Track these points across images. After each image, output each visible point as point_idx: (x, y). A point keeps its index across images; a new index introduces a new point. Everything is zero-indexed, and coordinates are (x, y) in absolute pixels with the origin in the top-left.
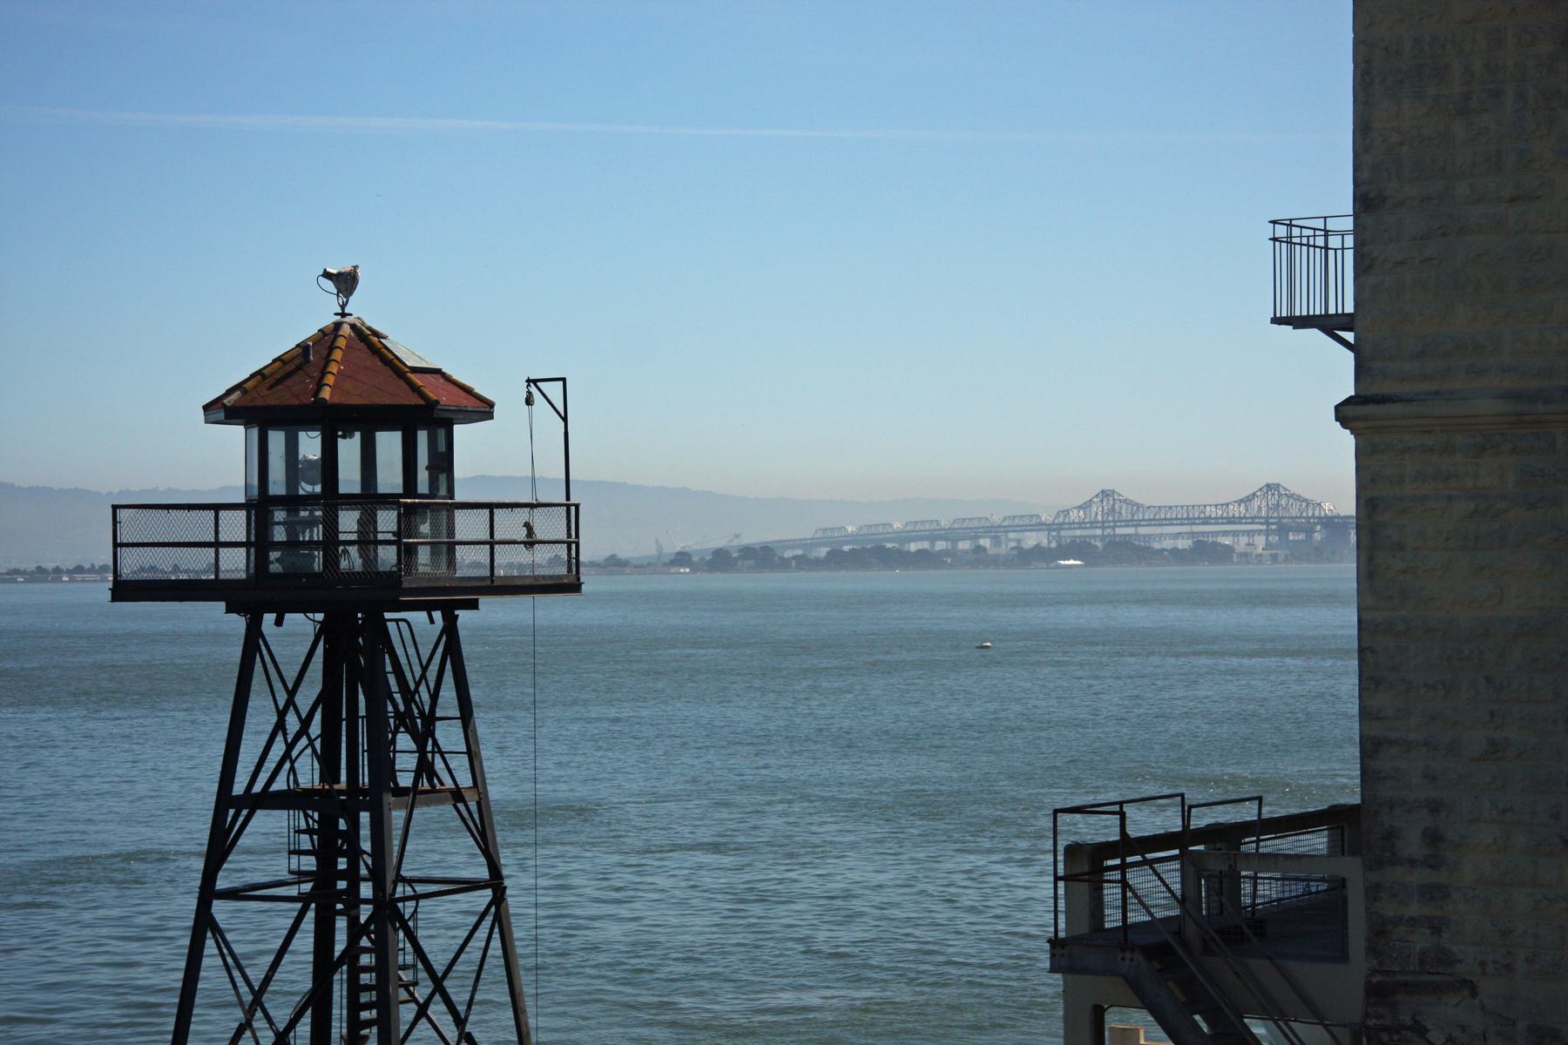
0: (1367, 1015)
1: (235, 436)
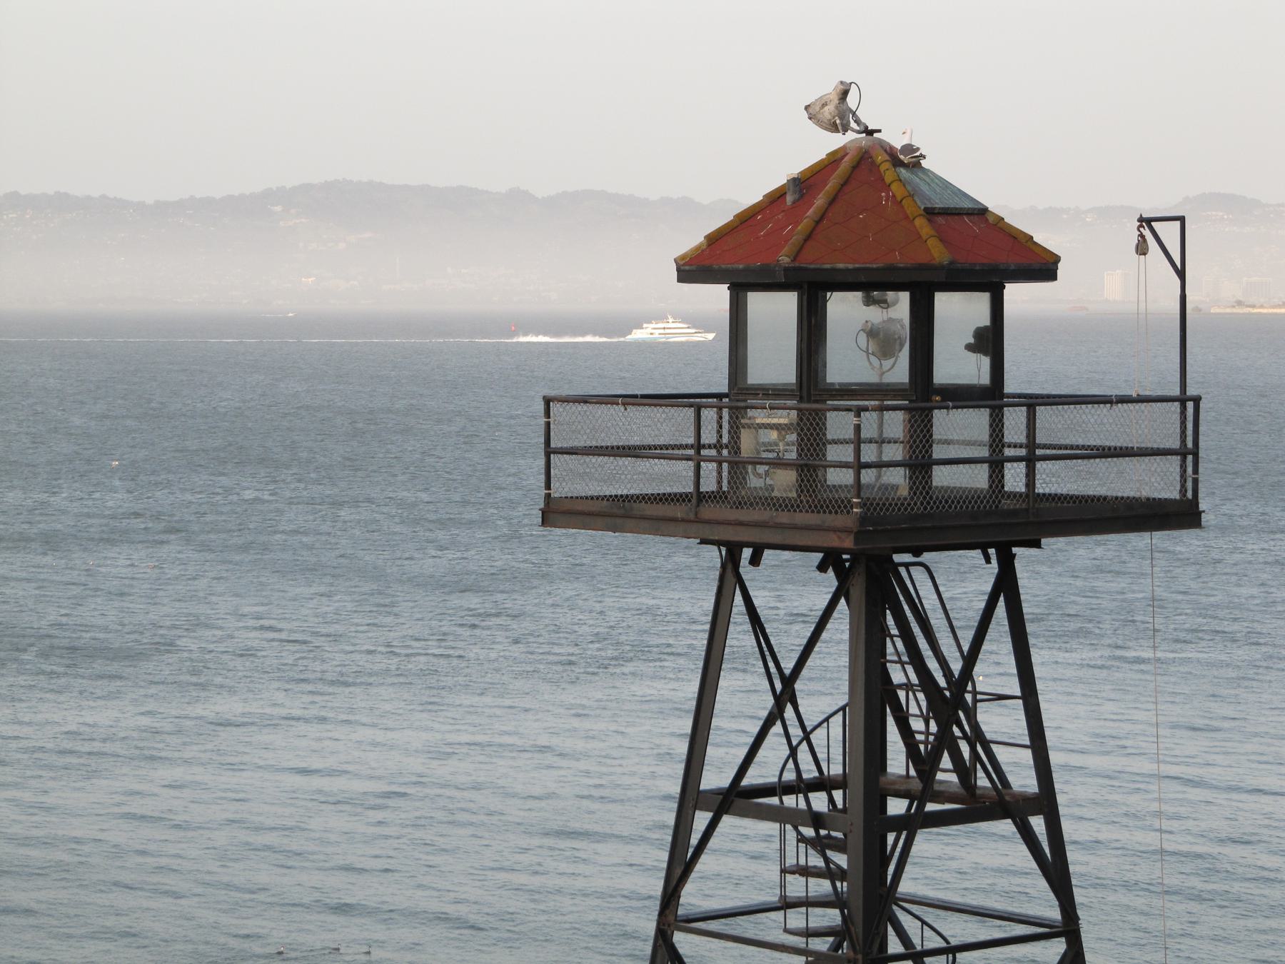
1: (717, 296)
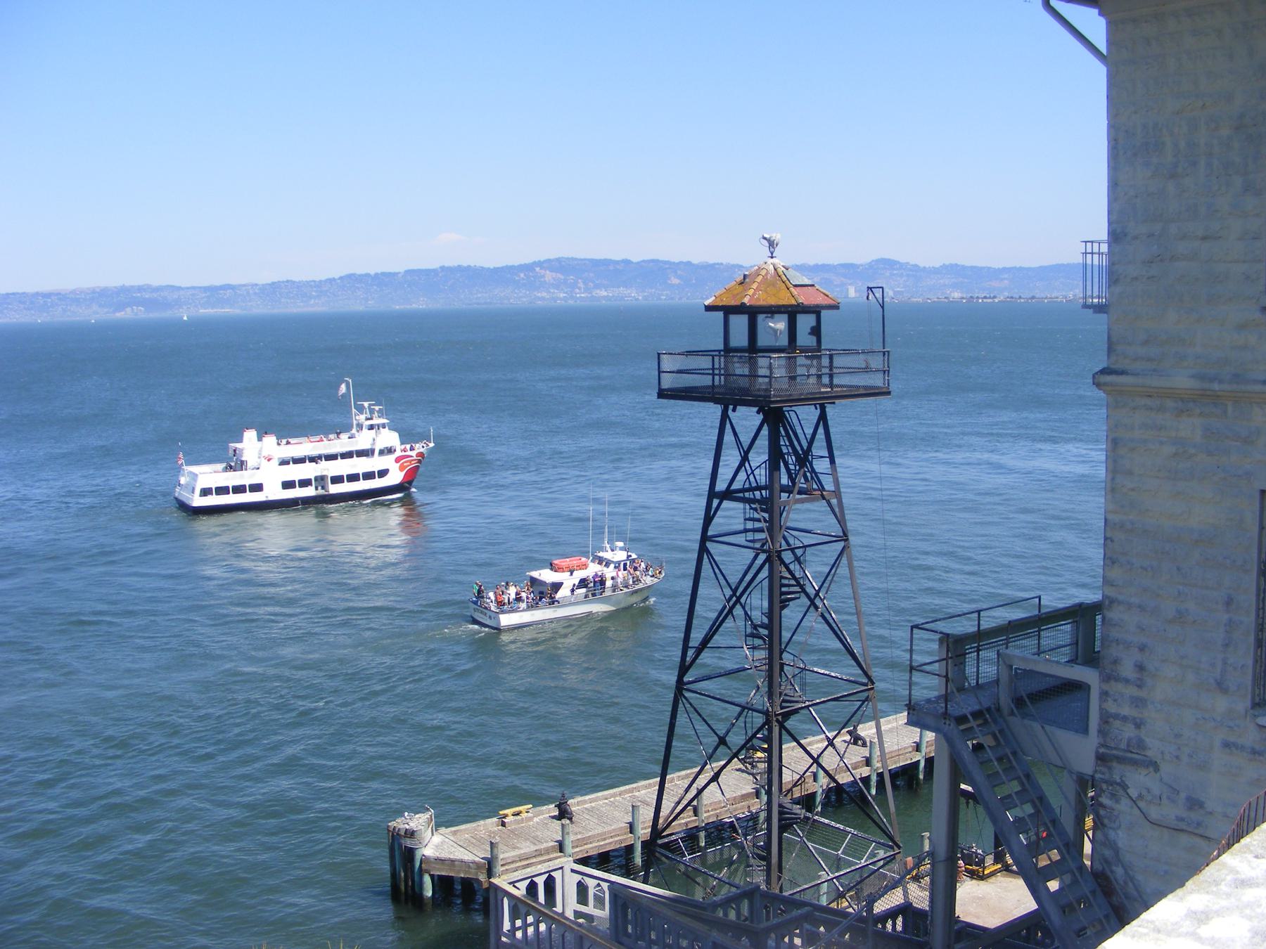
0: (1096, 771)
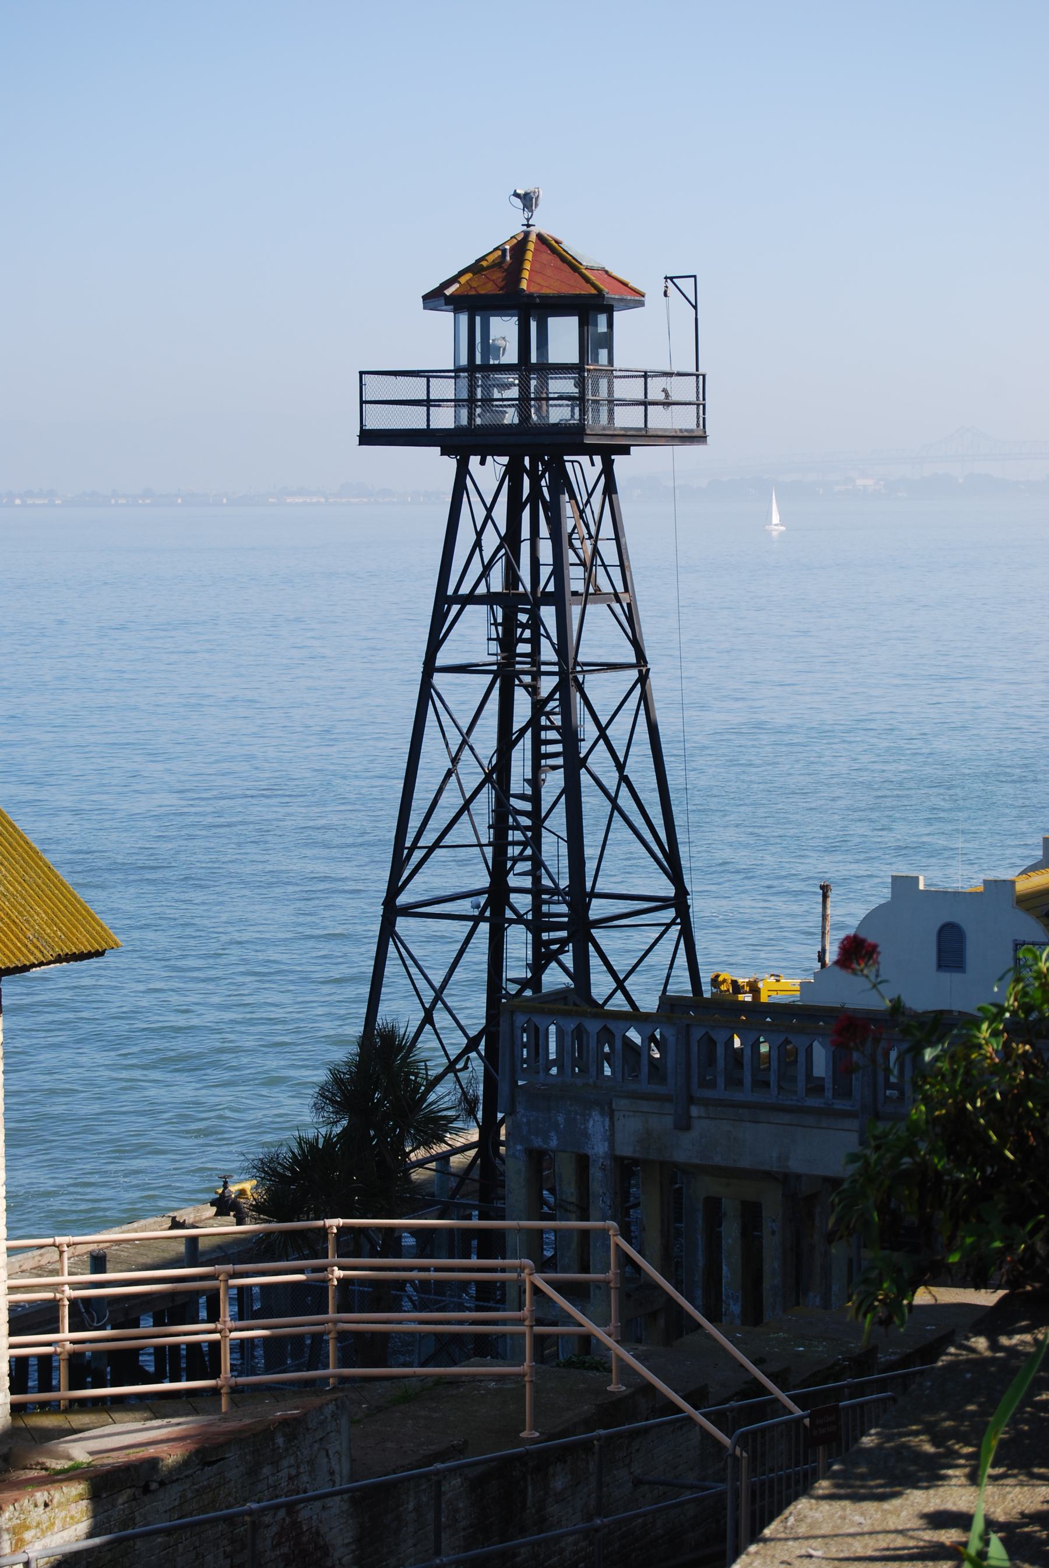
1: (445, 318)
